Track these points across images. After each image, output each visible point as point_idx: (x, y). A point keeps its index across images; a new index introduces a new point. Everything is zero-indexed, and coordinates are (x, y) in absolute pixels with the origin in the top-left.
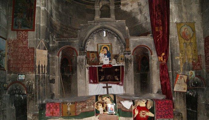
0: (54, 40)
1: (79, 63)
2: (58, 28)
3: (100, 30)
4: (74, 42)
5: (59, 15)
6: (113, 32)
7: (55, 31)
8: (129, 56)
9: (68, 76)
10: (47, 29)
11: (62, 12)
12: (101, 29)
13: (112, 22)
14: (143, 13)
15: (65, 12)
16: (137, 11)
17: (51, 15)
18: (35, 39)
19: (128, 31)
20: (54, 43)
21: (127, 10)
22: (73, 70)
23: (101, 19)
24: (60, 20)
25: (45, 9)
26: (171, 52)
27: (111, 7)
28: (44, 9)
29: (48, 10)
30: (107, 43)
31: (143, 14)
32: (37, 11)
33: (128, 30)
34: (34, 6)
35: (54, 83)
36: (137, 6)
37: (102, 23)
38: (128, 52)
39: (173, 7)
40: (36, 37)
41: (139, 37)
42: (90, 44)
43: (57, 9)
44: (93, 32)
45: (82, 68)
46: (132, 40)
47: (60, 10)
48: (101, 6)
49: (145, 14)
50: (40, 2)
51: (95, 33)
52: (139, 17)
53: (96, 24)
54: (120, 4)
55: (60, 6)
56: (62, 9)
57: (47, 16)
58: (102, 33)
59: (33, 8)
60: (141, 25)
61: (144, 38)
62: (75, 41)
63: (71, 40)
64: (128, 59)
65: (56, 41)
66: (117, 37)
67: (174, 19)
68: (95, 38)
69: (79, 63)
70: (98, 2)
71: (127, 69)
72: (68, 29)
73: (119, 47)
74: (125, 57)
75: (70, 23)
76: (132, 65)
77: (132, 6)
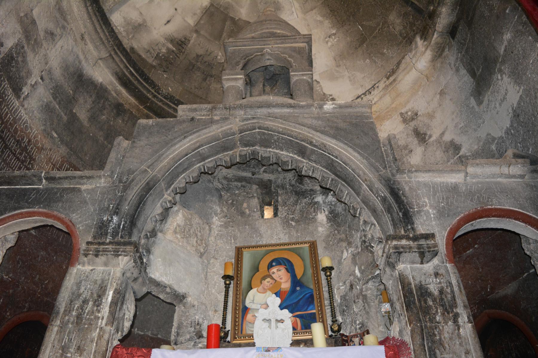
1: (68, 311)
4: (79, 190)
8: (429, 267)
11: (86, 123)
13: (302, 107)
14: (430, 136)
24: (62, 141)
30: (273, 242)
31: (432, 140)
36: (401, 127)
37: (251, 113)
42: (185, 232)
46: (425, 185)
47: (82, 113)
49: (443, 134)
53: (216, 118)
55: (81, 100)
56: (93, 118)
62: (84, 187)
63: (66, 178)
64: (424, 292)
68: (215, 219)
69: (68, 311)
74: (403, 280)
76: (467, 329)
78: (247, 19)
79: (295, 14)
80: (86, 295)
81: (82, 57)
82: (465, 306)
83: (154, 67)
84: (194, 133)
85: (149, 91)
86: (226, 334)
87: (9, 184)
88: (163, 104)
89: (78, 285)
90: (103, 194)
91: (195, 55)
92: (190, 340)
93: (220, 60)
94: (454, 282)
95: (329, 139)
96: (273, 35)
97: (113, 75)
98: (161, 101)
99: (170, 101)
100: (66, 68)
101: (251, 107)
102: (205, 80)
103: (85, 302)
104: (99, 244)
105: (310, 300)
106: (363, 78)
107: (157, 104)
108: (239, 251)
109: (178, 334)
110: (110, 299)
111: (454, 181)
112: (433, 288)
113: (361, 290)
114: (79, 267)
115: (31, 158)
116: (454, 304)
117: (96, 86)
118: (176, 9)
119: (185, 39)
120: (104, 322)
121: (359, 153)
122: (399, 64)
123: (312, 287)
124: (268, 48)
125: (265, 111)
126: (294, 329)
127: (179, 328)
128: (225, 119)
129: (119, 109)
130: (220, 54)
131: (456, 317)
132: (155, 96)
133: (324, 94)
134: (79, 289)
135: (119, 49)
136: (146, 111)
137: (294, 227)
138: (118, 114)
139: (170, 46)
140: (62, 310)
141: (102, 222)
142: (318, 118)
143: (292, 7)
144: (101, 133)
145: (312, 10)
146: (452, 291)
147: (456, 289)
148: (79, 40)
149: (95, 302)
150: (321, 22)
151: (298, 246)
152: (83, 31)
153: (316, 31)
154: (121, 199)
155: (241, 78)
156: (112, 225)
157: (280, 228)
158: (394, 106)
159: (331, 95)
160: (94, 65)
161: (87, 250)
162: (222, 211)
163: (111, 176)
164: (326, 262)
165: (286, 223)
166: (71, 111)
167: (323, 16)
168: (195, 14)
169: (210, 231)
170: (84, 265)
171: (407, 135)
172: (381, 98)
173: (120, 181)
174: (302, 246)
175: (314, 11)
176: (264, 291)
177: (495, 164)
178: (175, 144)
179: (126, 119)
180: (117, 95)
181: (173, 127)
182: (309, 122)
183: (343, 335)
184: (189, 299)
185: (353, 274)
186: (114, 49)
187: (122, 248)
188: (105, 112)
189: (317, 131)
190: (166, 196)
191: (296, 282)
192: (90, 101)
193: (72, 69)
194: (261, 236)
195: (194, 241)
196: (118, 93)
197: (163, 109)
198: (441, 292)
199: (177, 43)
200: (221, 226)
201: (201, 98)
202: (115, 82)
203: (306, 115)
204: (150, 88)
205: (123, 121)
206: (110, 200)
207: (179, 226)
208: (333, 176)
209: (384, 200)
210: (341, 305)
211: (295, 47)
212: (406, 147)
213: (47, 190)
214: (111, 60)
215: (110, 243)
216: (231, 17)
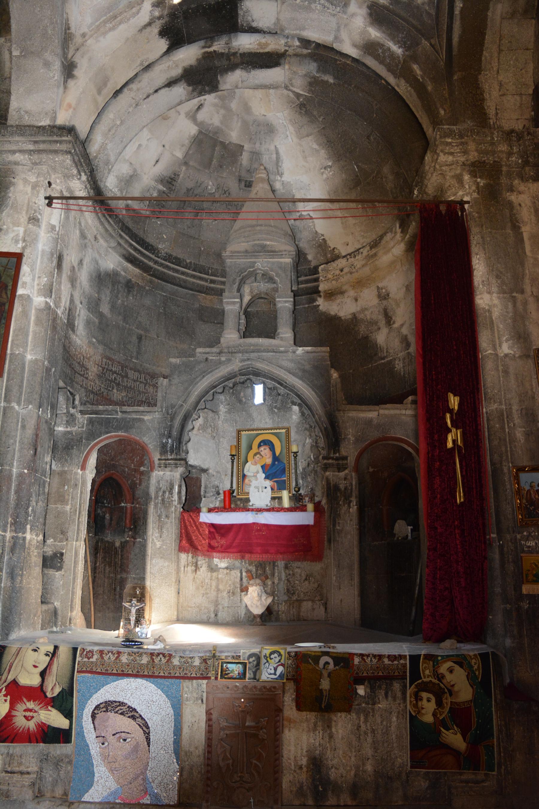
0: (72, 411)
1: (156, 497)
2: (93, 370)
3: (238, 379)
4: (143, 419)
5: (101, 327)
6: (285, 387)
7: (79, 379)
8: (342, 474)
9: (117, 544)
10: (48, 370)
11: (109, 316)
12: (243, 378)
13: (282, 352)
14: (394, 323)
15: (120, 317)
16: (374, 317)
17: (71, 325)
18: (2, 404)
19: (339, 386)
20: (71, 420)
21: (342, 314)
22: (137, 524)
23: (242, 340)
24: (99, 341)
25: (47, 303)
26: (493, 464)
27: (279, 301)
28: (43, 306)
29: (57, 306)
30: (262, 426)
32: (20, 309)
33: (339, 380)
34: (9, 293)
35: (60, 569)
36: (375, 301)
38: (337, 459)
39: (496, 301)
40: (6, 397)
41: (377, 407)
42: (203, 428)
43: (93, 305)
44: (215, 387)
45: (167, 517)
47: (105, 309)
48: (247, 299)
49: (402, 325)
50: (33, 280)
51: (219, 389)
52: (381, 338)
53: (223, 359)
54: (316, 291)
55: (103, 297)
56: (113, 307)
57: (54, 328)
58: (250, 390)
59: (4, 298)
60: (389, 367)
61: (398, 412)
62: (146, 418)
64: (336, 488)
65: (79, 415)
66: (299, 405)
67: (500, 346)
69: (156, 497)
70: (236, 286)
71: (334, 525)
72: (131, 374)
73: (308, 441)
75: (138, 353)
76: (354, 509)
77: (356, 300)
78: (239, 143)
79: (289, 137)
80: (164, 488)
81: (98, 257)
82: (356, 497)
83: (147, 217)
84: (209, 373)
85: (150, 259)
86: (233, 492)
87: (96, 414)
88: (164, 268)
89: (158, 482)
90: (159, 423)
91: (185, 190)
92: (214, 495)
93: (210, 190)
94: (354, 483)
95: (297, 380)
96: (264, 250)
97: (120, 256)
98: (161, 265)
99: (169, 262)
100: (91, 280)
101: (247, 352)
102: (197, 214)
103: (164, 492)
104: (165, 460)
105: (283, 471)
106: (355, 224)
107: (158, 270)
108: (239, 432)
109: (205, 492)
110: (177, 490)
111: (371, 416)
112: (342, 487)
113: (314, 467)
114: (157, 472)
115: (87, 369)
116: (350, 496)
117: (110, 275)
118: (164, 146)
119: (175, 174)
120: (176, 503)
121: (316, 392)
122: (381, 237)
123: (285, 462)
124: (259, 262)
125: (256, 354)
126: (272, 489)
127: (206, 487)
128: (229, 360)
129: (129, 286)
130: (211, 183)
131: (350, 502)
132: (156, 262)
133: (316, 232)
134: (159, 485)
135: (122, 231)
136: (149, 277)
137: (276, 414)
138: (129, 292)
139: (161, 187)
140: (153, 497)
141: (163, 444)
142: (292, 361)
143: (286, 130)
144: (120, 317)
145: (308, 136)
146: (352, 489)
147: (354, 487)
148: (93, 242)
149: (169, 492)
150: (317, 151)
151: (278, 431)
152: (96, 233)
153: (311, 159)
154: (171, 427)
155: (238, 302)
156: (169, 445)
157: (266, 414)
158: (374, 275)
159: (323, 235)
160: (106, 255)
161: (160, 464)
162: (226, 399)
163: (162, 411)
164: (294, 449)
165: (271, 409)
166: (99, 311)
167: (320, 145)
168: (183, 146)
169: (219, 418)
170: (159, 471)
171: (379, 311)
172: (363, 266)
173: (168, 414)
174: (281, 431)
175: (310, 138)
176: (256, 464)
177: (397, 409)
178: (198, 382)
179: (135, 293)
180: (125, 272)
181: (194, 367)
182: (286, 364)
183: (300, 494)
184: (210, 471)
185: (310, 457)
186: (120, 235)
187: (178, 462)
188: (120, 296)
189: (290, 373)
190: (194, 415)
191: (275, 458)
192: (108, 292)
193: (94, 275)
194: (253, 420)
195: (209, 430)
196: (125, 270)
197: (164, 273)
198: (346, 488)
199: (168, 182)
200: (226, 412)
201: (194, 238)
202: (122, 260)
203: (284, 358)
204: (151, 255)
205: (133, 297)
206: (164, 428)
207: (200, 425)
208: (300, 401)
209: (326, 429)
210: (302, 473)
211: (281, 263)
212: (376, 323)
213: (123, 419)
214: (119, 247)
215: (171, 459)
216: (221, 142)
